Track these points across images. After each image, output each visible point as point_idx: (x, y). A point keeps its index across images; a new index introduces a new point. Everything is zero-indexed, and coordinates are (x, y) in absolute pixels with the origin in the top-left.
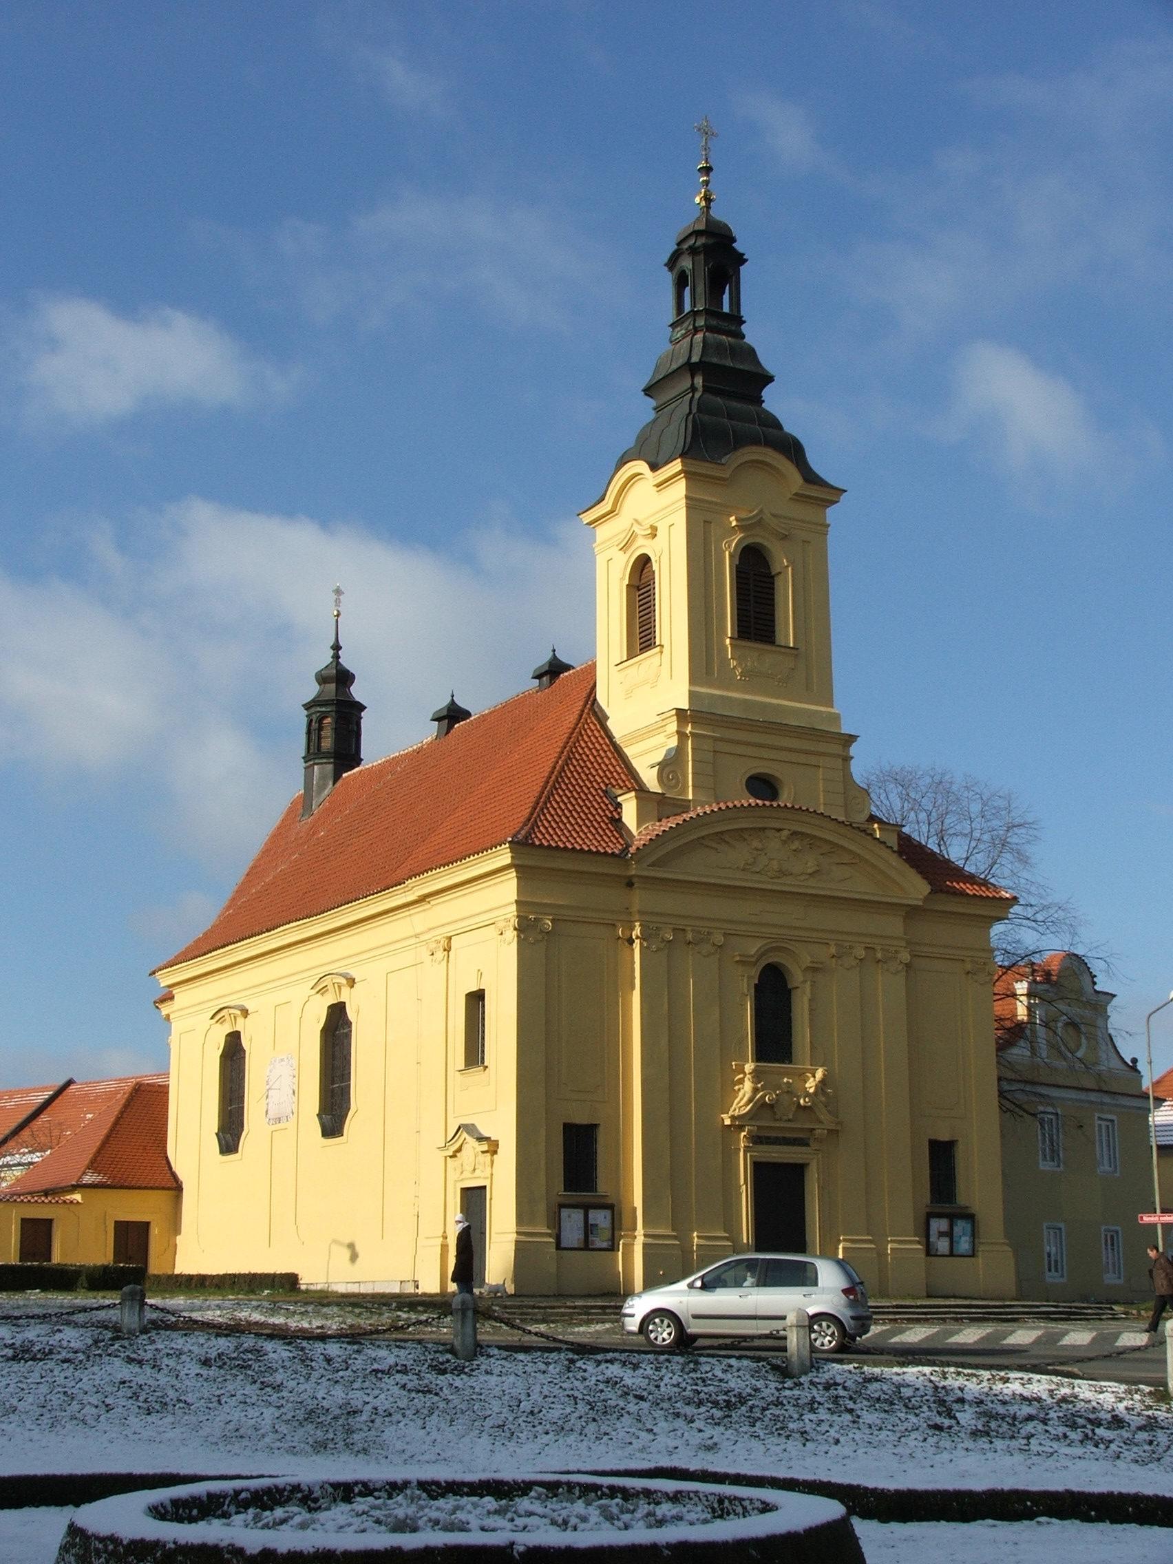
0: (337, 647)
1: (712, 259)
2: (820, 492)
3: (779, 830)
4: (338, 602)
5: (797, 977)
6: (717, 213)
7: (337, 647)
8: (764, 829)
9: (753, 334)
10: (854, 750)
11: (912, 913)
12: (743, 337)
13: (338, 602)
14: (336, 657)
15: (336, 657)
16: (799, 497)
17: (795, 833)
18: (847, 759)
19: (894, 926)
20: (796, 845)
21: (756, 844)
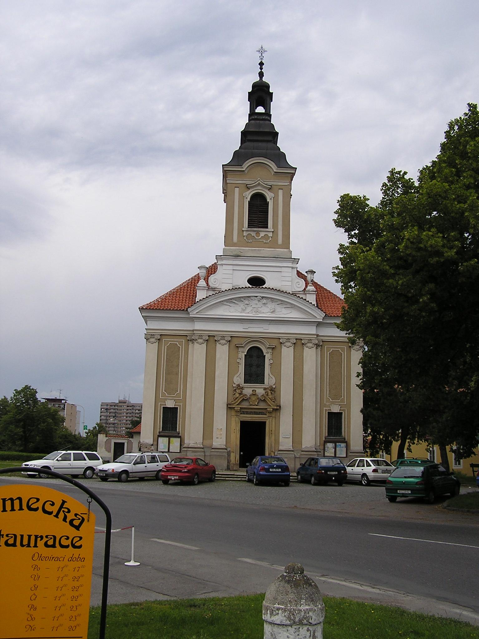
1: (260, 94)
3: (256, 297)
6: (264, 79)
8: (250, 297)
12: (270, 121)
17: (263, 297)
19: (312, 330)
20: (264, 301)
21: (247, 302)
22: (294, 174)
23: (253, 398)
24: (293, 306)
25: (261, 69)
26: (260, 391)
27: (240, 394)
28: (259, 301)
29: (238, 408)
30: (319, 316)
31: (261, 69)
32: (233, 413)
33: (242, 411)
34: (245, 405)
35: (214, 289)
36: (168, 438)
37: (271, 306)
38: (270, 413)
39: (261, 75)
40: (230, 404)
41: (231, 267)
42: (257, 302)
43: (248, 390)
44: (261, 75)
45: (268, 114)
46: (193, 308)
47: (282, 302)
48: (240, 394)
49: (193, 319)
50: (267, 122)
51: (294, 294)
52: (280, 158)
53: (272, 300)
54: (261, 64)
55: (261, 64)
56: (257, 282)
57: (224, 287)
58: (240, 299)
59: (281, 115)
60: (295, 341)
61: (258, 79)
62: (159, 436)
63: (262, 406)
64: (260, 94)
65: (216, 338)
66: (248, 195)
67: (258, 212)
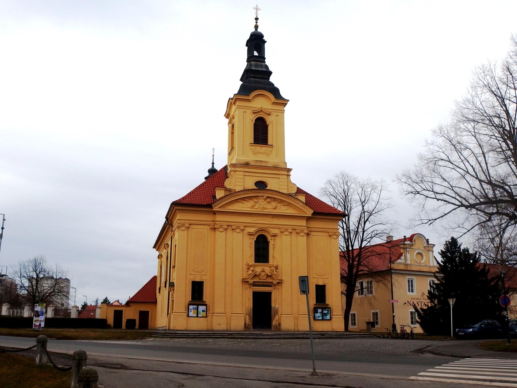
0: (213, 164)
1: (256, 42)
2: (284, 102)
4: (213, 152)
5: (269, 238)
6: (259, 30)
7: (213, 164)
8: (258, 196)
9: (268, 62)
10: (291, 173)
11: (308, 219)
13: (213, 152)
14: (213, 166)
15: (213, 166)
16: (274, 103)
17: (268, 197)
18: (289, 176)
19: (303, 223)
20: (269, 200)
21: (256, 200)
22: (286, 104)
23: (263, 274)
24: (289, 204)
25: (257, 22)
26: (267, 270)
27: (253, 271)
28: (265, 200)
29: (251, 281)
30: (309, 212)
31: (257, 22)
32: (247, 286)
33: (255, 284)
34: (256, 280)
35: (230, 190)
36: (196, 306)
37: (274, 204)
38: (275, 285)
39: (256, 27)
40: (245, 279)
41: (243, 173)
42: (263, 201)
43: (259, 268)
44: (256, 27)
45: (262, 58)
46: (216, 204)
47: (281, 201)
48: (253, 271)
49: (215, 213)
50: (263, 64)
51: (290, 195)
52: (275, 92)
53: (275, 199)
54: (257, 19)
55: (257, 19)
56: (261, 185)
57: (238, 189)
58: (250, 198)
59: (271, 59)
60: (291, 231)
61: (254, 30)
62: (189, 305)
63: (269, 280)
64: (256, 42)
65: (233, 227)
66: (254, 117)
67: (261, 132)
